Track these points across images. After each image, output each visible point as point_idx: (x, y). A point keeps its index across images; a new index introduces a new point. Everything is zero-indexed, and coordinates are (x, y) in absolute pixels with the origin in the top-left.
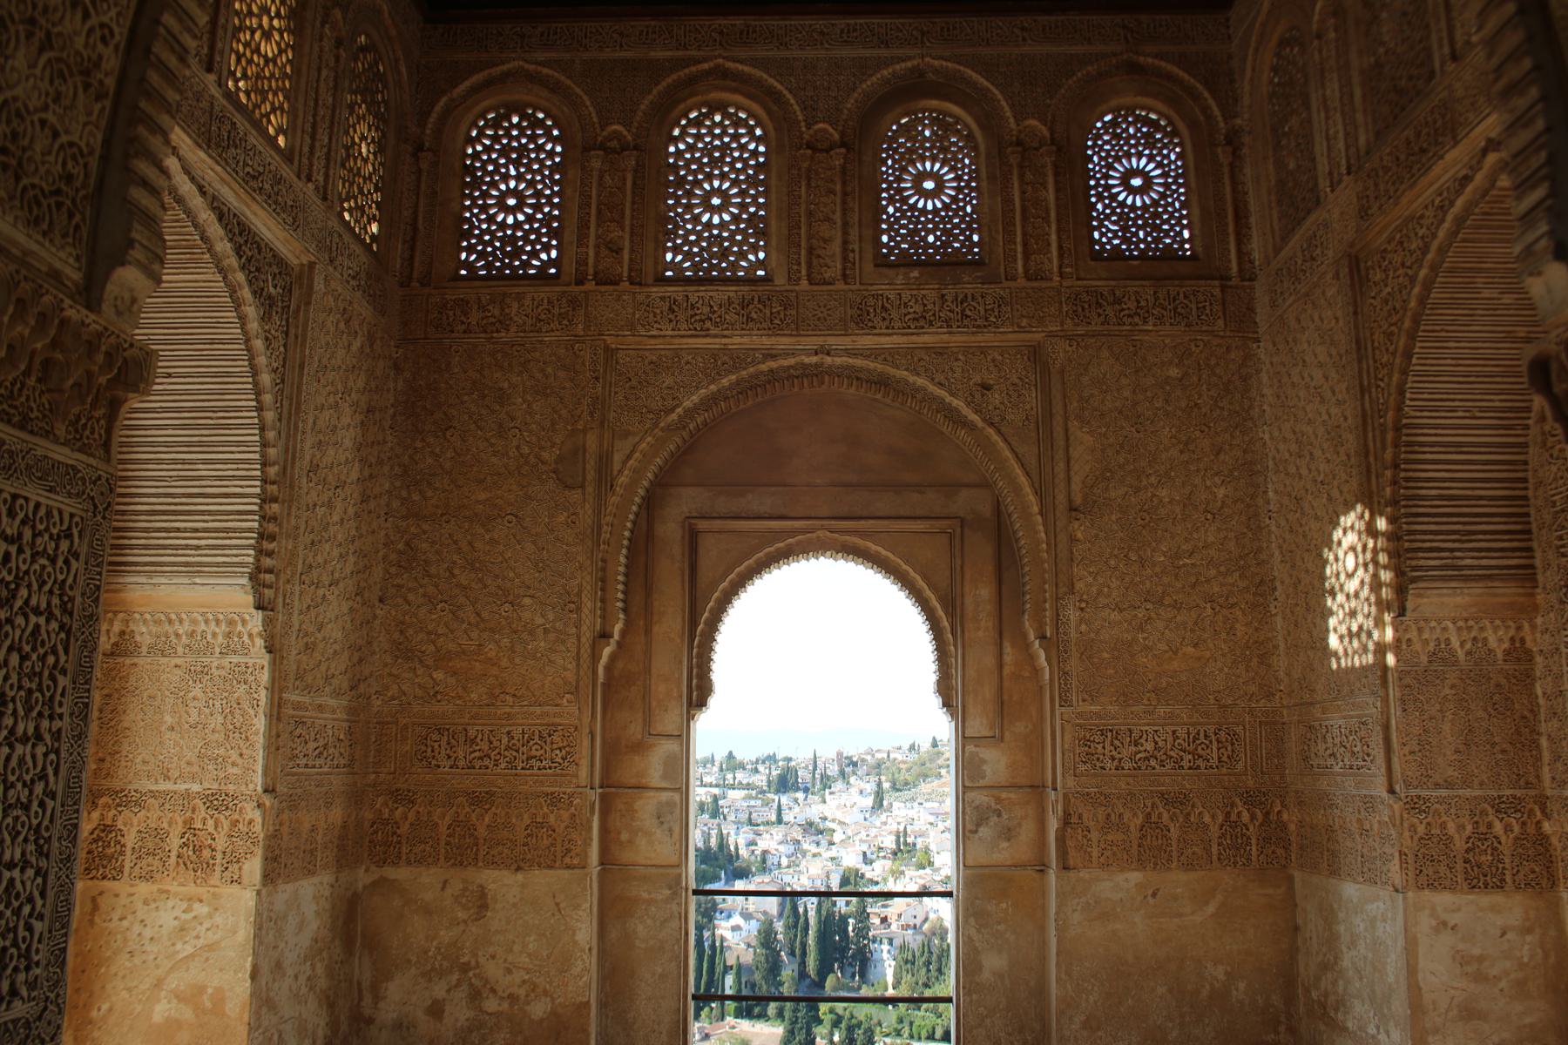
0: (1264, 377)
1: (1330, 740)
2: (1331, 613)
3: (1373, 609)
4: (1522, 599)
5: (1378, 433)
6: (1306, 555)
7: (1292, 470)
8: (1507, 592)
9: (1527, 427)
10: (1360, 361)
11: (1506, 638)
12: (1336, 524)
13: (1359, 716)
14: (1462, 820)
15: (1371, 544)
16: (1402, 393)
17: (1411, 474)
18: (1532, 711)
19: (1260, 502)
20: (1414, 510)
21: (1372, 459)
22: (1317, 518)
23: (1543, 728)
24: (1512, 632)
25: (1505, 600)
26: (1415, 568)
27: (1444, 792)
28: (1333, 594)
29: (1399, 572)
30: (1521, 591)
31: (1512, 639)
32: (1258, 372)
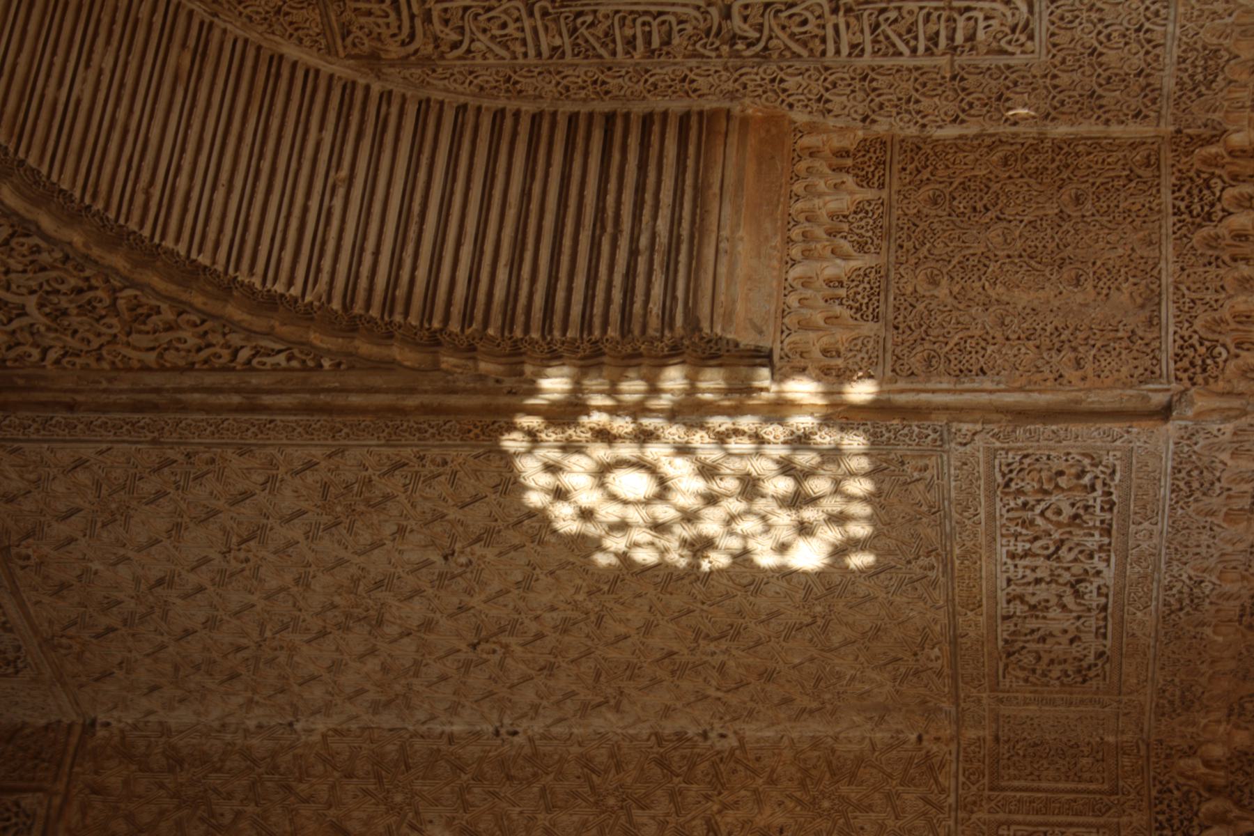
0: (182, 716)
1: (1042, 592)
2: (743, 557)
3: (747, 422)
4: (752, 140)
5: (353, 379)
6: (614, 628)
7: (408, 648)
8: (732, 162)
9: (386, 96)
10: (184, 408)
11: (836, 178)
12: (541, 518)
13: (991, 496)
14: (1228, 282)
15: (598, 419)
16: (272, 303)
17: (456, 310)
18: (991, 148)
19: (473, 751)
20: (537, 313)
21: (411, 401)
22: (526, 584)
23: (1028, 131)
24: (820, 165)
25: (751, 168)
26: (667, 320)
27: (1168, 311)
28: (702, 545)
29: (675, 353)
30: (733, 139)
31: (838, 169)
32: (165, 730)
